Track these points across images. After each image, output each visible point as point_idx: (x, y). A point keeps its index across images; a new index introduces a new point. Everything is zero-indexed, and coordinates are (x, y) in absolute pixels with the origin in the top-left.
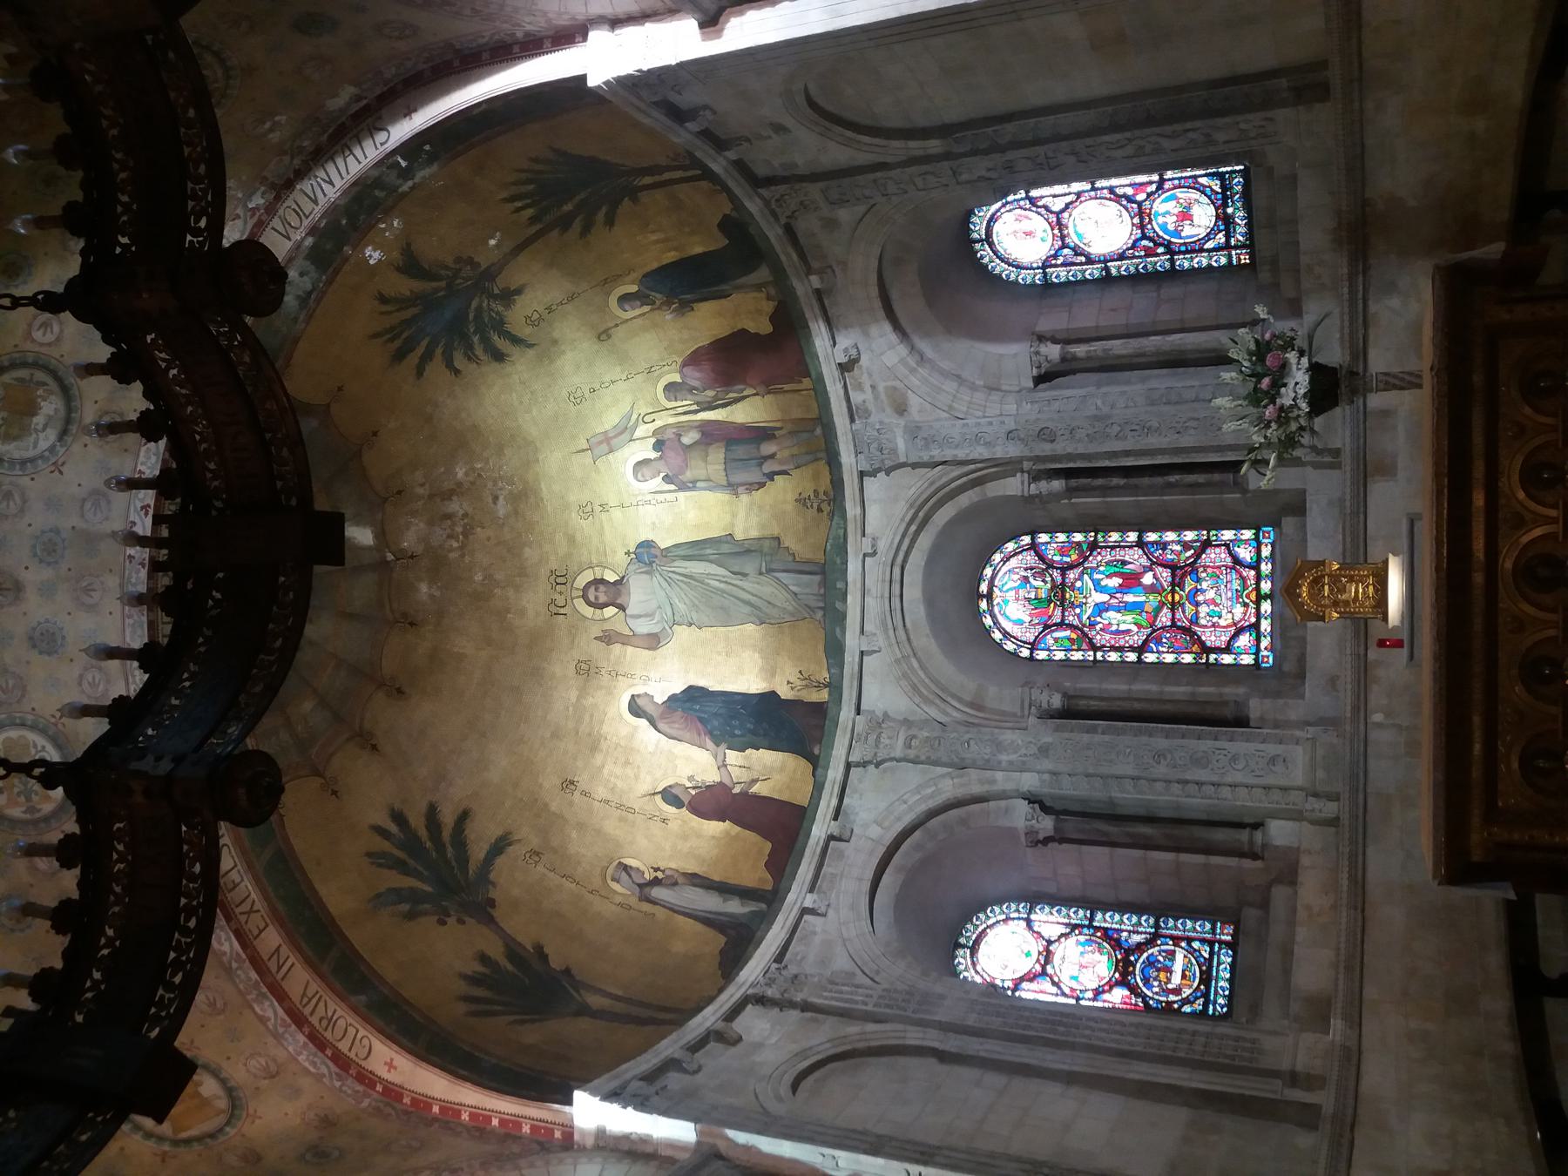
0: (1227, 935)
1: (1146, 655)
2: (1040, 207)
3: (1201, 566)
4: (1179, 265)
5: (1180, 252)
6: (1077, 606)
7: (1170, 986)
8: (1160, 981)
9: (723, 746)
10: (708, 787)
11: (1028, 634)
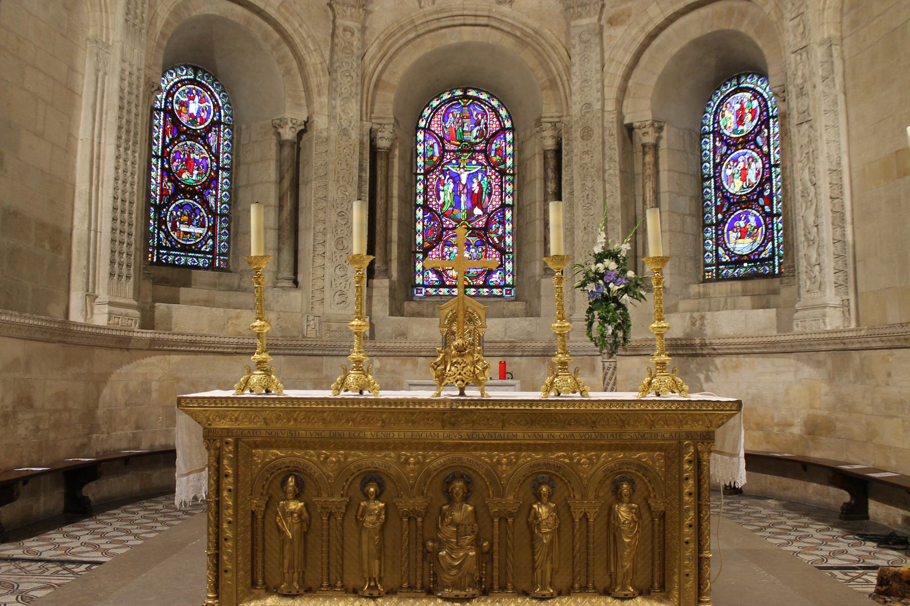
1: (422, 211)
2: (761, 127)
4: (707, 230)
5: (717, 230)
6: (457, 161)
7: (178, 223)
8: (181, 217)
11: (436, 125)
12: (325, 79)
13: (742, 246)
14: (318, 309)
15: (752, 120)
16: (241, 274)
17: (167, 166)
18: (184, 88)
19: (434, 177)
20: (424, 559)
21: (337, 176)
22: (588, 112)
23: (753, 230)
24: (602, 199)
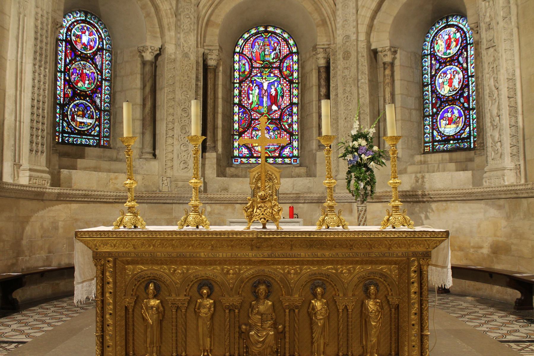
0: (104, 143)
1: (238, 107)
2: (462, 51)
3: (280, 132)
4: (426, 119)
6: (261, 74)
7: (75, 116)
11: (247, 51)
12: (173, 20)
13: (449, 129)
14: (169, 173)
15: (456, 46)
16: (118, 150)
17: (67, 78)
18: (78, 25)
19: (246, 85)
20: (239, 337)
21: (181, 84)
22: (347, 41)
23: (457, 119)
24: (357, 99)
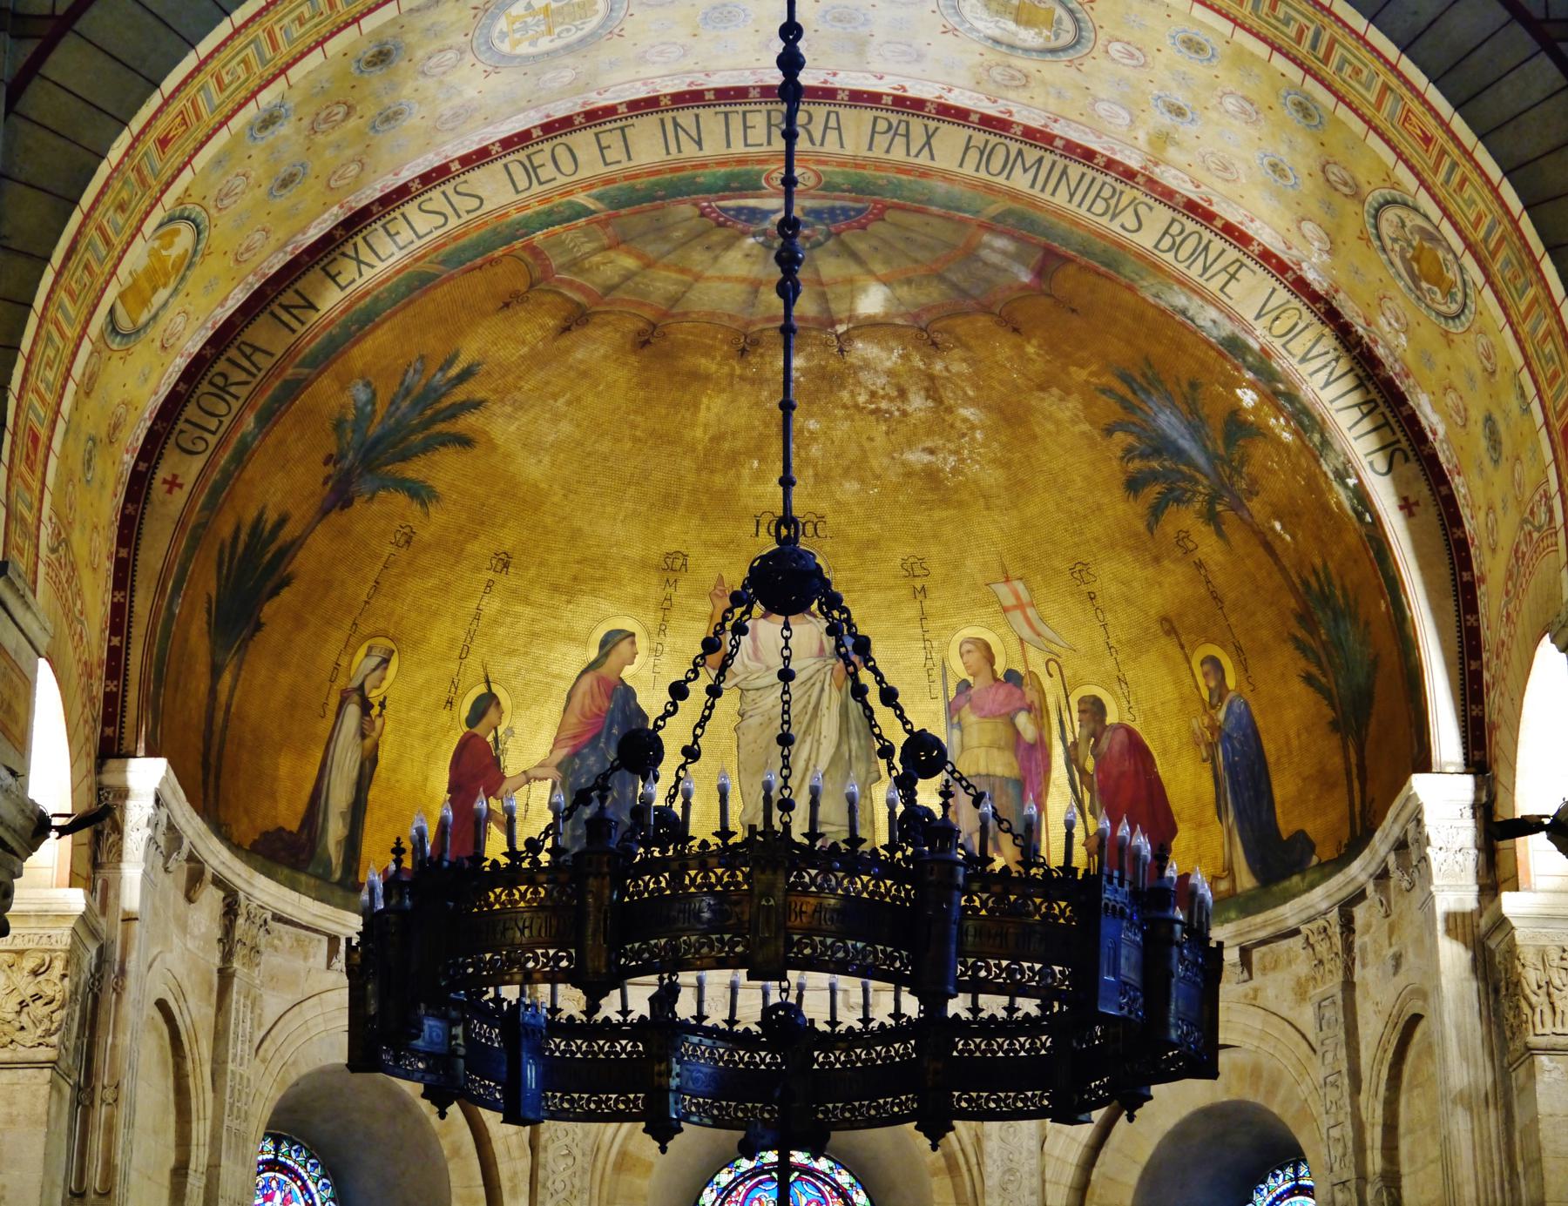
9: (557, 774)
10: (497, 760)
